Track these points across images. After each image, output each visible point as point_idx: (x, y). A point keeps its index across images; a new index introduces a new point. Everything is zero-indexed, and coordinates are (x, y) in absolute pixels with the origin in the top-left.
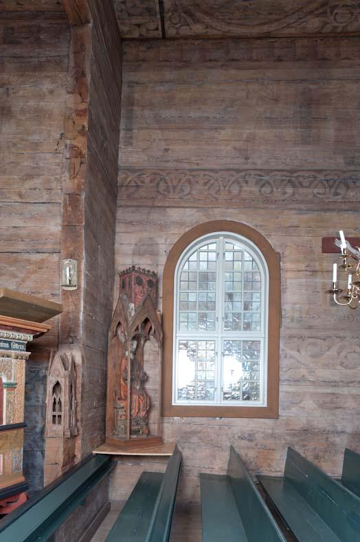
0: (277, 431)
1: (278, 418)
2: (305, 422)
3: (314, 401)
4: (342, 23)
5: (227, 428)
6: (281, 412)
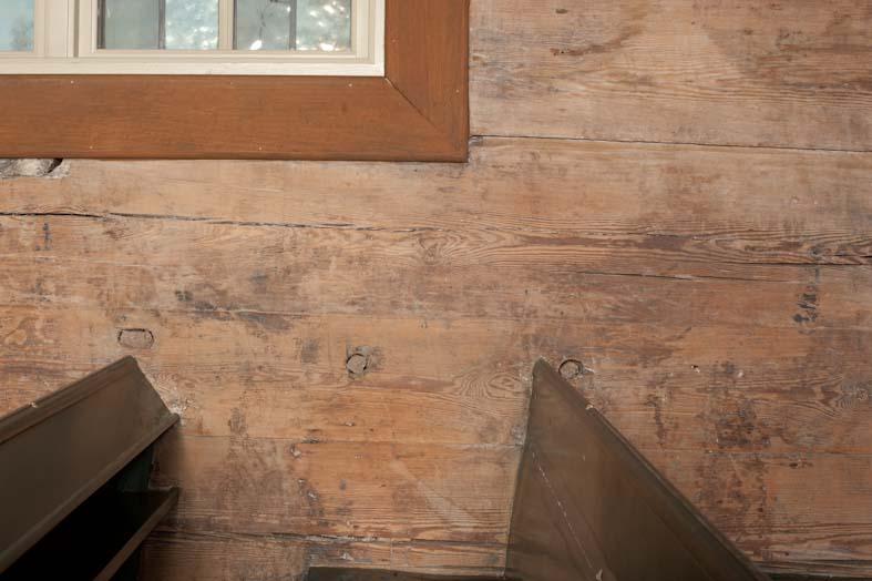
0: (454, 250)
1: (462, 161)
2: (656, 183)
3: (719, 37)
5: (95, 230)
6: (483, 111)
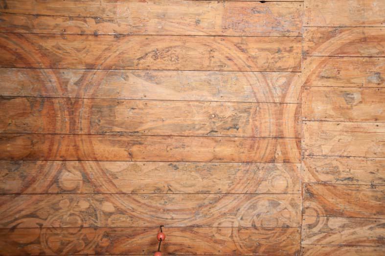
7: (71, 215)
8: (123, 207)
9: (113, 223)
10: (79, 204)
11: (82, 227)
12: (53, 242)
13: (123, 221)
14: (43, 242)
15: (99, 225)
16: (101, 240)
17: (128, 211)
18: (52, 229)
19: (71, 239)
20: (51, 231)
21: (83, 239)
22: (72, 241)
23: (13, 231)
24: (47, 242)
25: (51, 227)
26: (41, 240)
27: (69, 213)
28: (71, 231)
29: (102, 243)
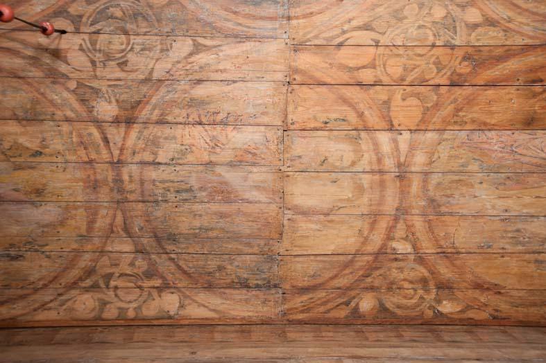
4: (130, 302)
7: (420, 27)
8: (495, 16)
9: (478, 40)
10: (432, 11)
11: (433, 46)
12: (393, 66)
13: (494, 37)
14: (380, 66)
15: (457, 43)
16: (460, 64)
17: (501, 22)
18: (392, 48)
19: (417, 63)
20: (391, 51)
21: (434, 63)
22: (419, 66)
23: (339, 50)
24: (384, 65)
25: (391, 44)
26: (377, 63)
27: (417, 25)
28: (419, 51)
29: (461, 68)
